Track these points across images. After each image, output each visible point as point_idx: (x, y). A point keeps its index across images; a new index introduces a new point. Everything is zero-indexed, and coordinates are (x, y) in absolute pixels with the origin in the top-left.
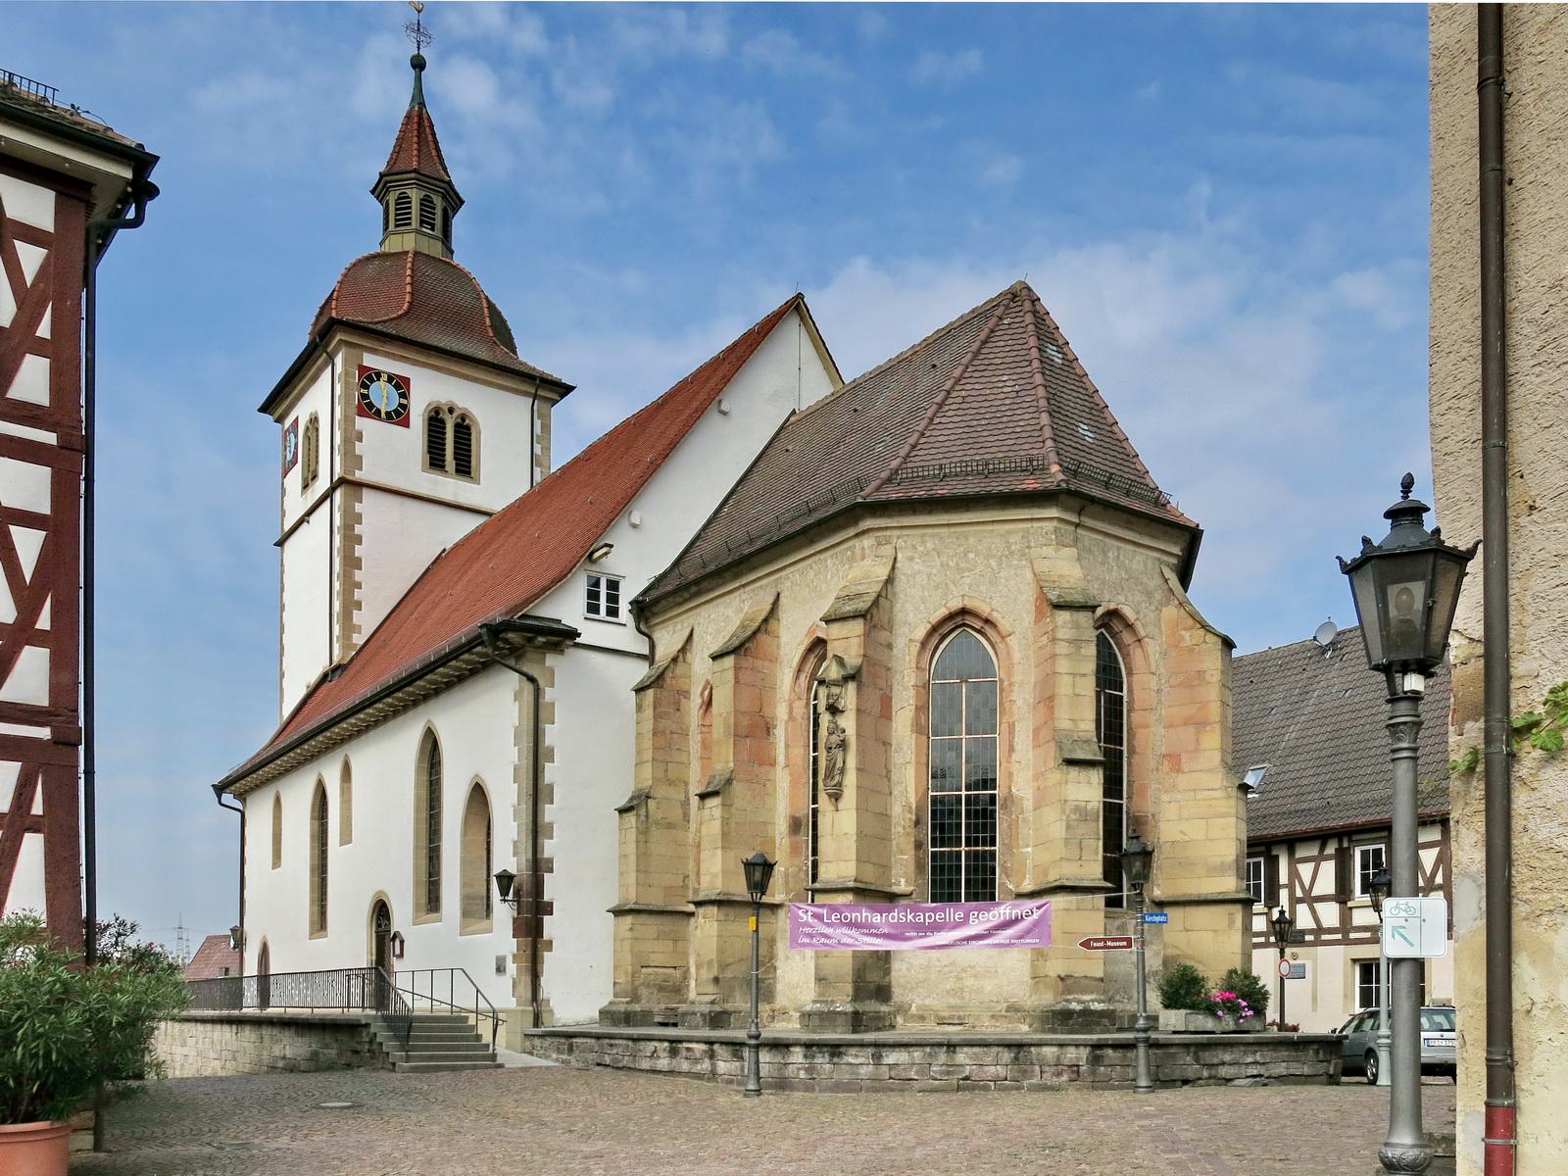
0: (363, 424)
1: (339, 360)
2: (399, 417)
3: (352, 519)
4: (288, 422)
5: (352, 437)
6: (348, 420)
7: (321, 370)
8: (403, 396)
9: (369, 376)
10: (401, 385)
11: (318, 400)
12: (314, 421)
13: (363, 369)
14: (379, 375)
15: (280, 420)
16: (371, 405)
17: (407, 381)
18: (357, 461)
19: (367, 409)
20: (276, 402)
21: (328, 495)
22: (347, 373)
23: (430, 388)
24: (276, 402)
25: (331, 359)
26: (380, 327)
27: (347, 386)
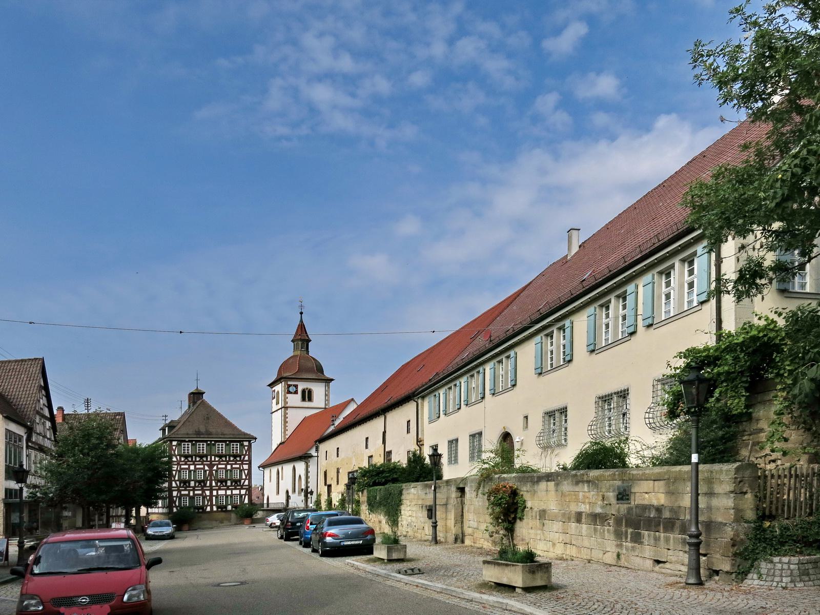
0: (288, 395)
1: (283, 383)
2: (296, 392)
3: (286, 414)
4: (273, 389)
5: (286, 398)
6: (285, 395)
7: (279, 384)
8: (297, 388)
9: (289, 386)
10: (296, 386)
11: (279, 388)
12: (278, 392)
13: (288, 385)
14: (291, 385)
15: (272, 388)
16: (290, 391)
17: (297, 385)
18: (287, 403)
19: (289, 392)
20: (272, 385)
21: (281, 408)
22: (285, 386)
23: (302, 386)
24: (272, 385)
25: (281, 383)
26: (290, 377)
27: (284, 389)
